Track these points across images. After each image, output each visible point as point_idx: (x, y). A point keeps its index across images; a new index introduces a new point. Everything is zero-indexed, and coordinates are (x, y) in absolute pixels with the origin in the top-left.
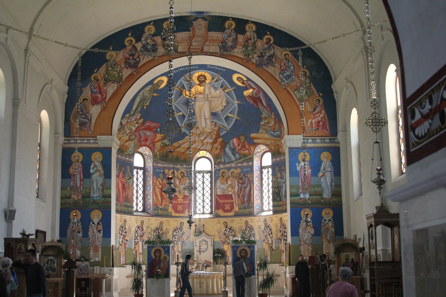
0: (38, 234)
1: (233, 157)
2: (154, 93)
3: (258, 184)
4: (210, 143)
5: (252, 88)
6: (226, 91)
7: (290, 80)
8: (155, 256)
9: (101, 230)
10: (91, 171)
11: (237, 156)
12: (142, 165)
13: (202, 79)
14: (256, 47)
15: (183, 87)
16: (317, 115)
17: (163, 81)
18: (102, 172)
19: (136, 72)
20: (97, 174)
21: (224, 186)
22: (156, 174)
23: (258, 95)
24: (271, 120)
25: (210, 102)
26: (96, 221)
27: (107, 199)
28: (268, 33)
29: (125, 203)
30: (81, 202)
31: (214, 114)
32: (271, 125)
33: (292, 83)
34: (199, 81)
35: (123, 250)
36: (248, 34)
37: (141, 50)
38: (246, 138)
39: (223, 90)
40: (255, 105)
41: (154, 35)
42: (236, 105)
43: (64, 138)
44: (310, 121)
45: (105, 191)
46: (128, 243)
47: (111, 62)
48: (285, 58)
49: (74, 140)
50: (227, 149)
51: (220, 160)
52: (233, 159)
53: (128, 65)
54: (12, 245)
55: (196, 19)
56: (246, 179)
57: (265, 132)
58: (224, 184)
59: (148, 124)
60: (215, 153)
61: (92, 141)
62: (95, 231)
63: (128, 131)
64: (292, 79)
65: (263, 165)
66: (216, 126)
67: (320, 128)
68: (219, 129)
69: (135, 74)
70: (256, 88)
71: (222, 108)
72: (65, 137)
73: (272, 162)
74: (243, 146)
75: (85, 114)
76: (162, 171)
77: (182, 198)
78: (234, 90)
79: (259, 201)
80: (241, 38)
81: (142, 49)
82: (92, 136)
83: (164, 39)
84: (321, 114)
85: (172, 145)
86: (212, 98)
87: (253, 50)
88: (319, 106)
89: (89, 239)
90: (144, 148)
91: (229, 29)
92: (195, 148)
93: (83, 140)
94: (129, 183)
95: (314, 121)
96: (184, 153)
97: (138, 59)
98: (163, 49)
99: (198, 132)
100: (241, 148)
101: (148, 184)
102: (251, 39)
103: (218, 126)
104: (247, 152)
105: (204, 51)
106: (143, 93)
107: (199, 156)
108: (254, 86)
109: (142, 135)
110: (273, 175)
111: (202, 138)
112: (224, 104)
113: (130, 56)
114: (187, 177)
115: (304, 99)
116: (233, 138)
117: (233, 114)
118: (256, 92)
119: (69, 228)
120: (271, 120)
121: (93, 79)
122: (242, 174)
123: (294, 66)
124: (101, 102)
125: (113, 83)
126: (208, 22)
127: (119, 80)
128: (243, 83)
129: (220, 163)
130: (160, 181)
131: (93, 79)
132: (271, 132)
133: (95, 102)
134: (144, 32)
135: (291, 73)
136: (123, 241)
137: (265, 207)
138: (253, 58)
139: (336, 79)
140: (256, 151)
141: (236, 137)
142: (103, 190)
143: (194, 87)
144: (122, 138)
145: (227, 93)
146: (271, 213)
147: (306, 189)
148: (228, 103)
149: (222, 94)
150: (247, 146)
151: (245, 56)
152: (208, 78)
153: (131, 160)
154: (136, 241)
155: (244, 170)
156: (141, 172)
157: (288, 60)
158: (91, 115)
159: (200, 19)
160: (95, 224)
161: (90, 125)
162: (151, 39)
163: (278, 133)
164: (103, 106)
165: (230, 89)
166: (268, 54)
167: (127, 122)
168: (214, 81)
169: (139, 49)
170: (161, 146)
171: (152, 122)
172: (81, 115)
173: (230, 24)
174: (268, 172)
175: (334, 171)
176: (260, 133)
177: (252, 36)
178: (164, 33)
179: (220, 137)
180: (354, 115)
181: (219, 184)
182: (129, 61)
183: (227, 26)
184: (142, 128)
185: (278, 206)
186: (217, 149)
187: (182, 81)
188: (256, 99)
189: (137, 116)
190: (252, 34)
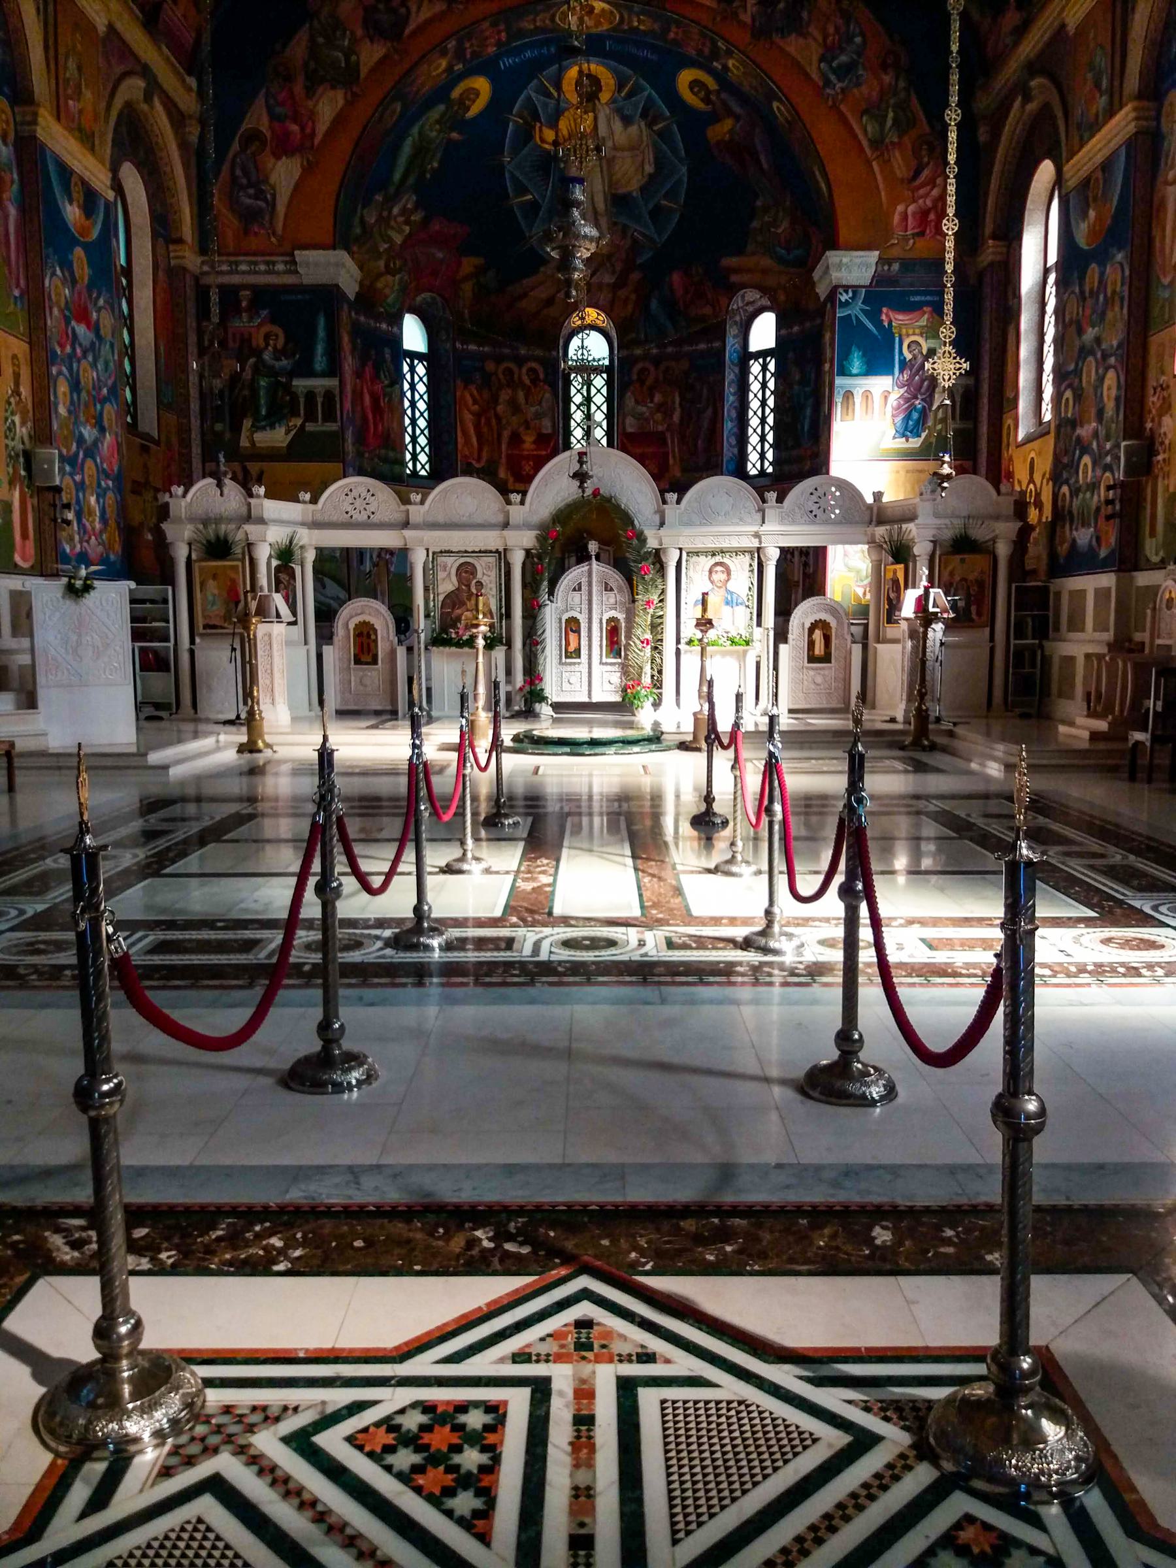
2: (452, 129)
3: (736, 404)
4: (608, 285)
5: (730, 113)
6: (655, 128)
7: (850, 80)
15: (536, 117)
16: (922, 192)
17: (477, 93)
21: (644, 409)
29: (383, 452)
33: (855, 90)
39: (650, 125)
42: (684, 169)
49: (230, 264)
50: (654, 304)
51: (634, 335)
59: (437, 227)
69: (396, 57)
77: (534, 442)
79: (736, 451)
93: (256, 263)
94: (390, 395)
97: (403, 10)
103: (629, 235)
104: (708, 310)
106: (422, 126)
108: (737, 109)
112: (649, 169)
120: (781, 214)
123: (862, 34)
125: (333, 88)
127: (347, 77)
128: (706, 100)
129: (637, 343)
130: (475, 392)
132: (778, 249)
133: (284, 148)
135: (855, 57)
138: (745, 7)
143: (566, 114)
145: (660, 134)
148: (659, 163)
153: (395, 329)
156: (421, 370)
158: (273, 188)
163: (797, 252)
167: (380, 219)
168: (623, 94)
181: (630, 401)
187: (533, 95)
189: (407, 201)
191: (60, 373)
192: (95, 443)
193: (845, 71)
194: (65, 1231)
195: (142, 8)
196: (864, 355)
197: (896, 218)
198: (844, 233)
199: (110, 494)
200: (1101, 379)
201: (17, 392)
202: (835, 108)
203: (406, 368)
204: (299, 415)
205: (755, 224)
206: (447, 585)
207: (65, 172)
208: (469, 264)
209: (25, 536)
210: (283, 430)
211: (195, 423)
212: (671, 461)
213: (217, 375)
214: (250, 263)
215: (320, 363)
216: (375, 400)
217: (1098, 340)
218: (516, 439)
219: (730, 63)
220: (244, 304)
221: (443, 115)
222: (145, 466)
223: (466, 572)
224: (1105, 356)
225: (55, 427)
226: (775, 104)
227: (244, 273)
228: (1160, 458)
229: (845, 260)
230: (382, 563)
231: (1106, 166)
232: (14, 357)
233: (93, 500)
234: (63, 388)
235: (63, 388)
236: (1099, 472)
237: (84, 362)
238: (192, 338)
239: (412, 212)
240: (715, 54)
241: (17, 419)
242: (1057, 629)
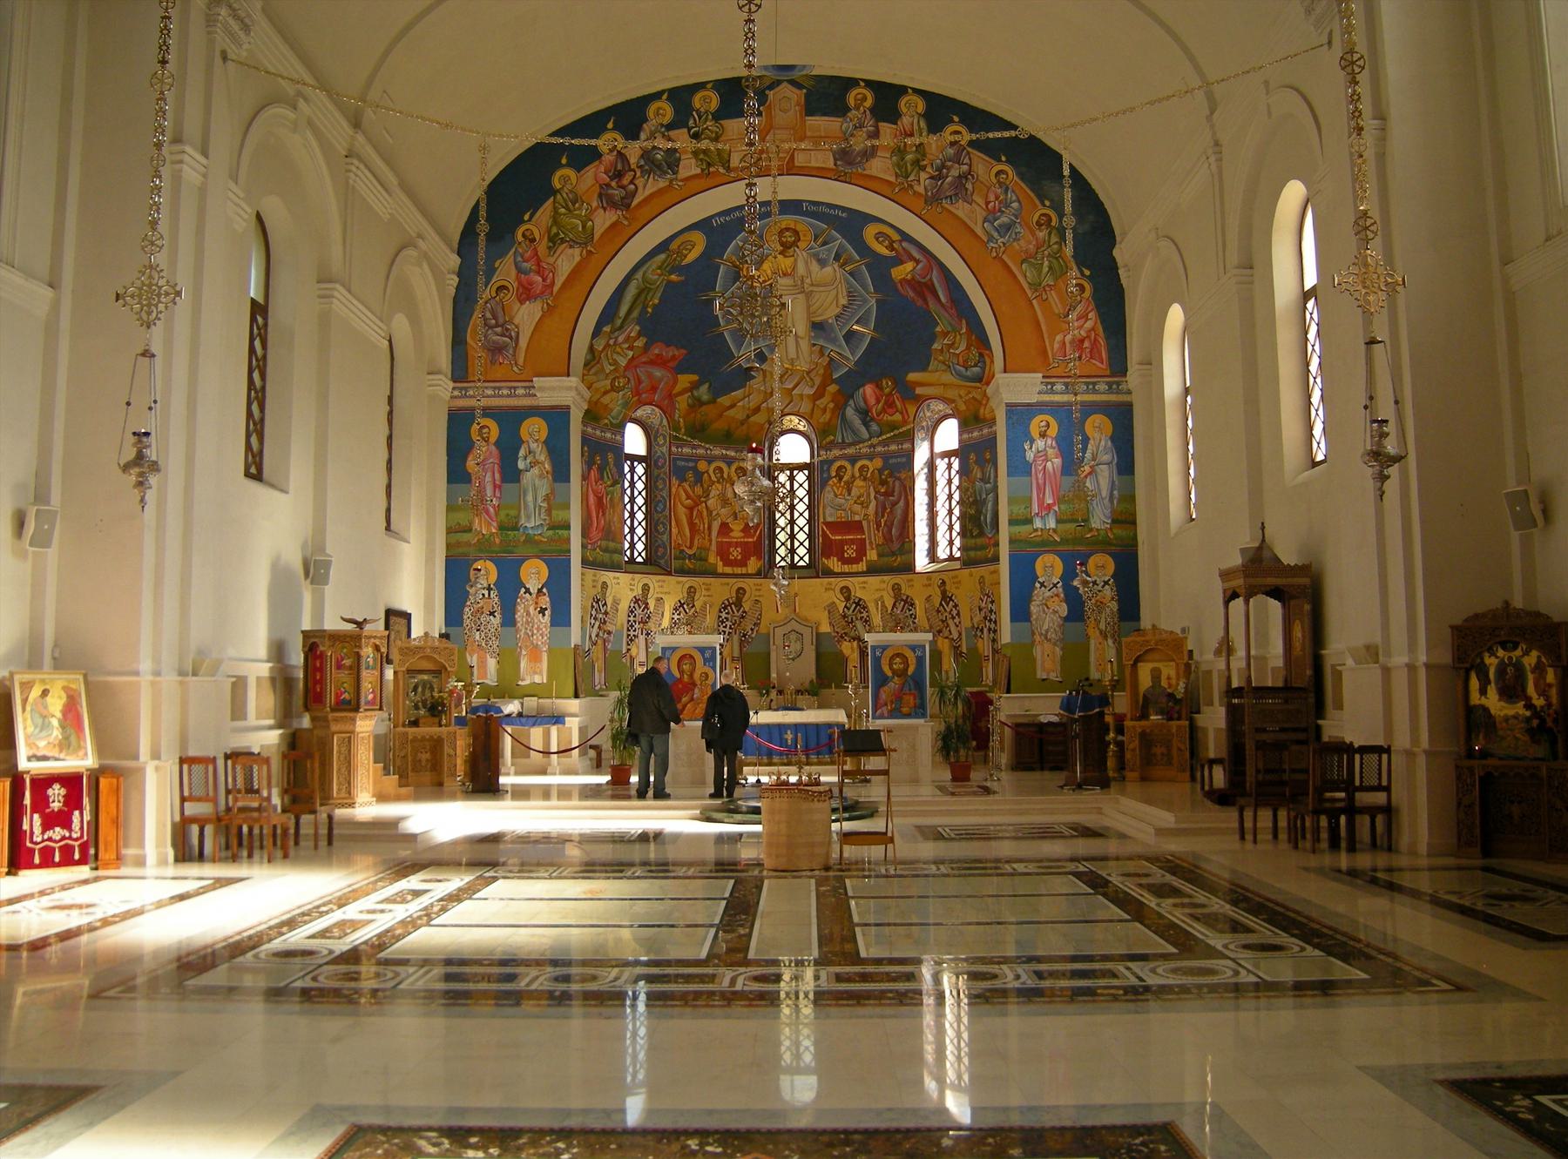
0: (393, 619)
1: (863, 429)
4: (809, 396)
5: (912, 258)
8: (681, 672)
9: (546, 609)
10: (521, 465)
11: (875, 427)
13: (789, 239)
14: (924, 155)
18: (546, 466)
19: (626, 218)
20: (535, 471)
23: (929, 277)
24: (958, 337)
25: (809, 295)
26: (533, 586)
27: (560, 532)
28: (956, 119)
29: (604, 543)
30: (497, 541)
31: (818, 327)
32: (957, 352)
33: (1015, 244)
34: (782, 244)
35: (601, 656)
36: (906, 121)
37: (638, 162)
38: (895, 383)
39: (841, 267)
40: (920, 302)
41: (670, 127)
42: (874, 301)
43: (451, 385)
44: (1059, 338)
45: (554, 513)
46: (612, 638)
47: (565, 195)
48: (999, 181)
50: (850, 412)
52: (866, 435)
54: (322, 648)
55: (774, 84)
56: (897, 483)
57: (944, 367)
59: (657, 351)
60: (822, 420)
61: (521, 391)
62: (531, 609)
63: (609, 368)
64: (1016, 233)
65: (937, 450)
66: (822, 354)
67: (1084, 357)
68: (829, 363)
69: (626, 223)
70: (925, 260)
71: (838, 310)
72: (454, 382)
73: (960, 441)
74: (890, 405)
75: (502, 326)
77: (742, 531)
81: (642, 163)
84: (1087, 320)
85: (713, 401)
86: (812, 285)
87: (916, 163)
88: (1084, 301)
89: (517, 631)
91: (857, 108)
93: (499, 388)
95: (1069, 338)
97: (632, 187)
98: (693, 161)
100: (883, 408)
101: (659, 498)
102: (912, 135)
104: (897, 417)
105: (797, 164)
109: (643, 378)
111: (791, 386)
112: (844, 301)
113: (612, 180)
115: (1044, 283)
116: (863, 385)
117: (865, 325)
118: (922, 269)
119: (468, 603)
120: (958, 337)
121: (520, 238)
122: (886, 472)
123: (1019, 202)
124: (542, 293)
125: (571, 247)
126: (805, 91)
127: (585, 239)
128: (893, 249)
130: (689, 489)
131: (520, 238)
133: (526, 294)
134: (646, 120)
136: (601, 634)
137: (942, 552)
138: (919, 181)
139: (1124, 234)
141: (870, 382)
142: (549, 511)
144: (594, 385)
147: (1049, 507)
148: (851, 295)
149: (838, 277)
150: (897, 403)
151: (897, 176)
152: (805, 236)
153: (618, 437)
154: (632, 633)
155: (892, 461)
156: (640, 470)
157: (1004, 188)
158: (517, 327)
159: (785, 84)
160: (530, 594)
161: (515, 352)
162: (664, 136)
164: (548, 304)
166: (955, 172)
167: (607, 345)
169: (633, 160)
170: (688, 405)
171: (668, 346)
172: (491, 327)
173: (859, 96)
174: (950, 466)
175: (1117, 464)
176: (932, 372)
177: (916, 127)
178: (695, 120)
179: (834, 381)
180: (1176, 316)
181: (828, 495)
182: (610, 191)
183: (851, 102)
184: (644, 360)
185: (975, 548)
186: (824, 410)
188: (923, 288)
189: (632, 330)
190: (916, 121)
194: (428, 1139)
203: (627, 469)
205: (936, 346)
208: (685, 380)
212: (868, 547)
218: (725, 529)
227: (488, 396)
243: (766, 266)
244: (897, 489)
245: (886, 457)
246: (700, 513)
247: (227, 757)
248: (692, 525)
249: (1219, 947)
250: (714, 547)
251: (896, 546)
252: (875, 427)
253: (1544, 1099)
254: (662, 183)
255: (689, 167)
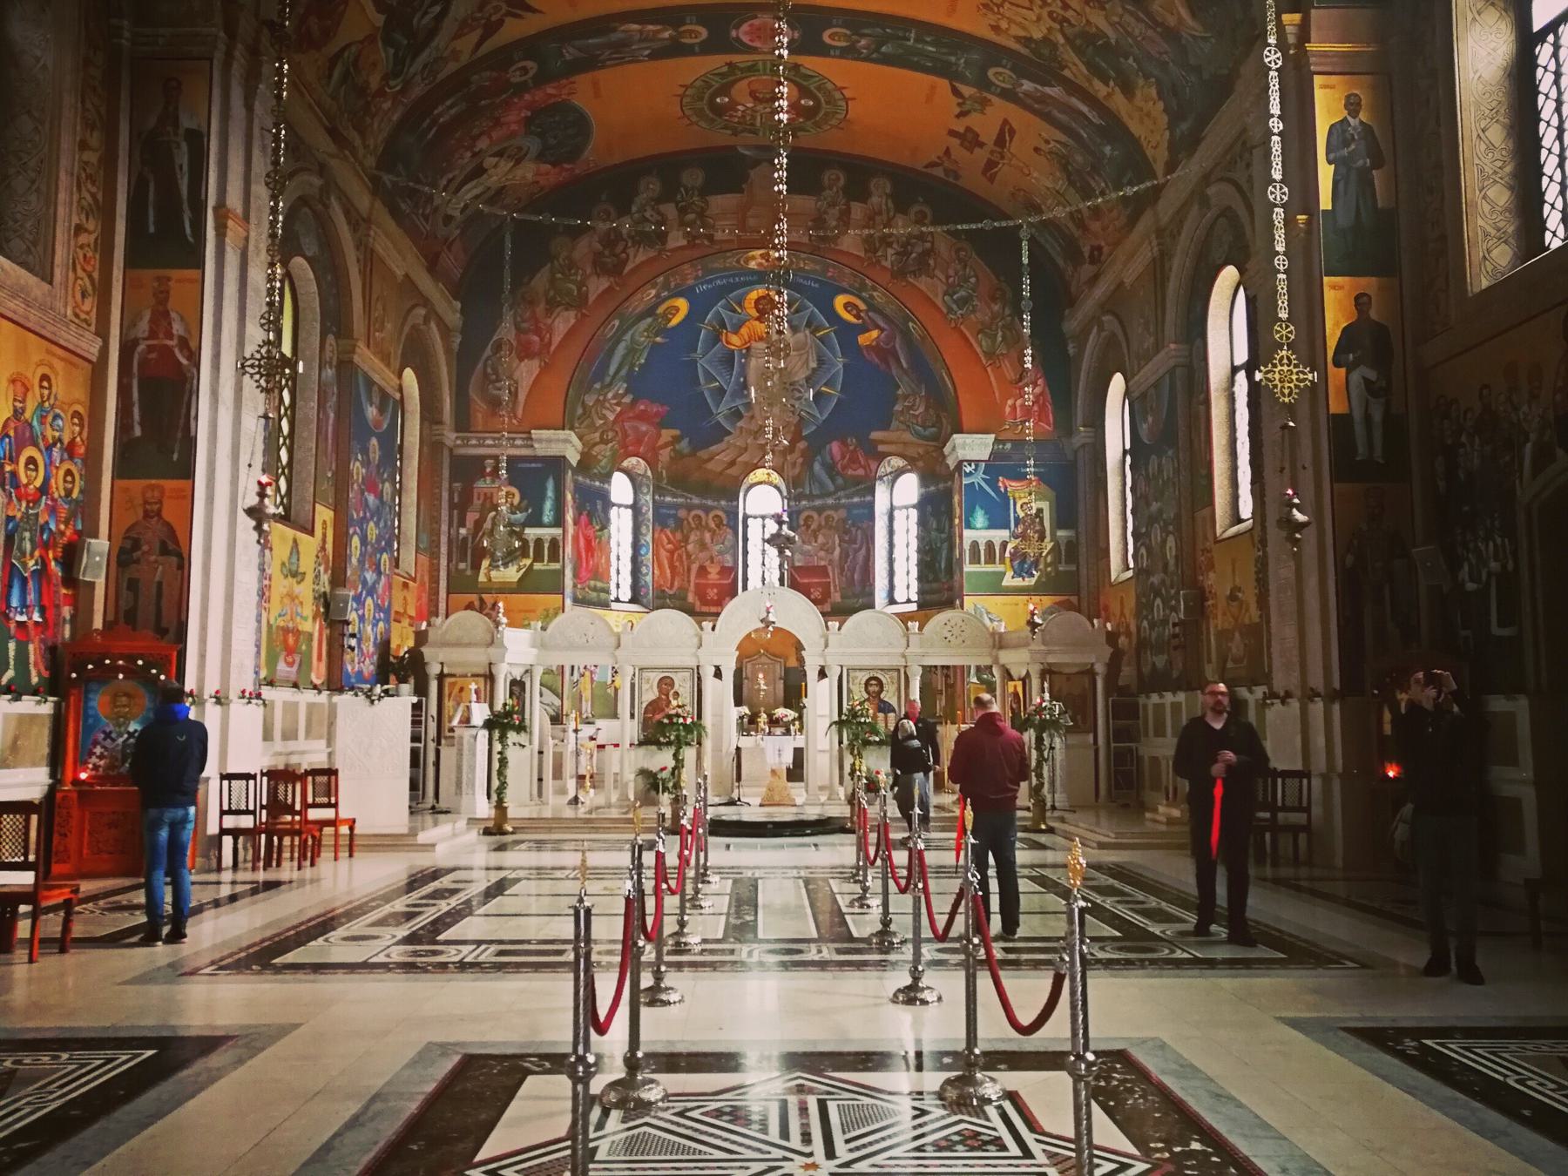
1: (828, 482)
5: (877, 327)
11: (840, 481)
12: (630, 501)
15: (723, 325)
17: (677, 310)
19: (617, 284)
21: (809, 548)
22: (660, 520)
29: (592, 583)
35: (588, 686)
36: (875, 200)
39: (813, 333)
40: (883, 367)
44: (1010, 402)
46: (598, 670)
49: (478, 439)
50: (817, 467)
52: (832, 488)
53: (600, 268)
56: (859, 532)
57: (904, 427)
58: (810, 543)
59: (642, 407)
61: (518, 442)
71: (808, 373)
74: (854, 460)
76: (672, 512)
77: (718, 573)
78: (835, 332)
80: (857, 210)
82: (521, 429)
83: (683, 211)
85: (693, 454)
90: (633, 460)
92: (746, 463)
94: (600, 537)
95: (1019, 402)
96: (721, 473)
99: (754, 427)
102: (880, 213)
104: (861, 472)
107: (755, 481)
109: (629, 432)
110: (922, 523)
112: (813, 365)
114: (727, 525)
116: (830, 442)
118: (887, 336)
123: (976, 276)
125: (567, 309)
127: (580, 302)
128: (858, 317)
133: (525, 353)
137: (900, 595)
140: (881, 471)
145: (820, 339)
146: (913, 607)
148: (821, 361)
151: (866, 251)
155: (855, 512)
156: (627, 515)
165: (828, 330)
183: (826, 181)
185: (933, 592)
188: (884, 352)
191: (355, 533)
192: (374, 584)
193: (963, 302)
195: (426, 257)
196: (986, 513)
197: (1008, 410)
198: (967, 419)
199: (381, 624)
200: (1164, 542)
201: (323, 548)
202: (956, 328)
204: (528, 557)
205: (898, 408)
206: (651, 695)
207: (370, 383)
208: (667, 434)
209: (320, 659)
210: (516, 567)
211: (444, 562)
213: (462, 524)
214: (494, 439)
215: (548, 516)
216: (588, 542)
217: (1160, 511)
218: (703, 571)
219: (875, 294)
220: (488, 470)
221: (650, 326)
222: (405, 598)
223: (666, 684)
224: (1166, 524)
225: (349, 573)
226: (911, 324)
227: (489, 446)
228: (1210, 602)
229: (968, 441)
230: (587, 674)
231: (1156, 385)
232: (325, 522)
233: (369, 628)
234: (356, 541)
235: (356, 541)
236: (1167, 612)
237: (372, 524)
238: (445, 495)
239: (623, 396)
240: (863, 287)
241: (322, 569)
242: (1147, 735)
243: (744, 331)
244: (859, 537)
245: (849, 507)
246: (680, 556)
247: (263, 774)
248: (673, 568)
249: (1158, 933)
250: (692, 587)
251: (858, 589)
252: (840, 481)
253: (1428, 1042)
254: (652, 253)
255: (676, 240)
